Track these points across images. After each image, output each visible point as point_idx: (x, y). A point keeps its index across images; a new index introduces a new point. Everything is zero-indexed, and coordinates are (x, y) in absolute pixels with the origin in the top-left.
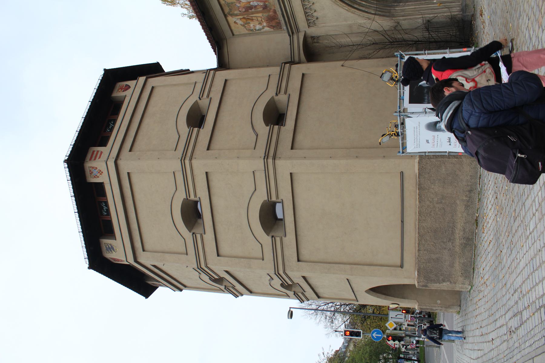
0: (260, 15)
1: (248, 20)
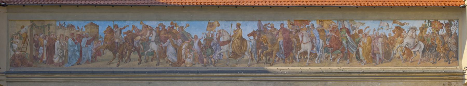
0: (28, 52)
1: (24, 39)
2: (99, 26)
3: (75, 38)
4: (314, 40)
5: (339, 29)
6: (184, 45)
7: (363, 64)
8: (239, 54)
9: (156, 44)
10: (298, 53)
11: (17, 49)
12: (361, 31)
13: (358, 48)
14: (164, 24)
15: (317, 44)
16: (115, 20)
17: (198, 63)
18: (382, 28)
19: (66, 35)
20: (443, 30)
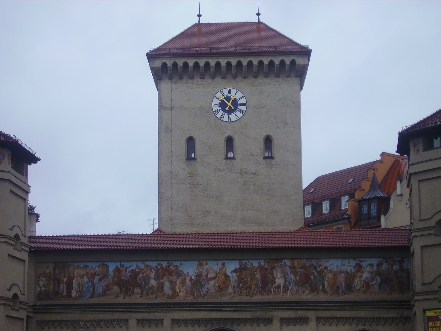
0: (51, 288)
2: (109, 266)
3: (89, 276)
4: (287, 275)
5: (308, 266)
6: (178, 281)
7: (328, 296)
8: (223, 288)
9: (156, 281)
10: (273, 287)
11: (42, 285)
12: (326, 268)
13: (324, 282)
14: (162, 264)
15: (289, 280)
16: (121, 261)
17: (190, 296)
18: (345, 265)
19: (82, 273)
20: (396, 266)
